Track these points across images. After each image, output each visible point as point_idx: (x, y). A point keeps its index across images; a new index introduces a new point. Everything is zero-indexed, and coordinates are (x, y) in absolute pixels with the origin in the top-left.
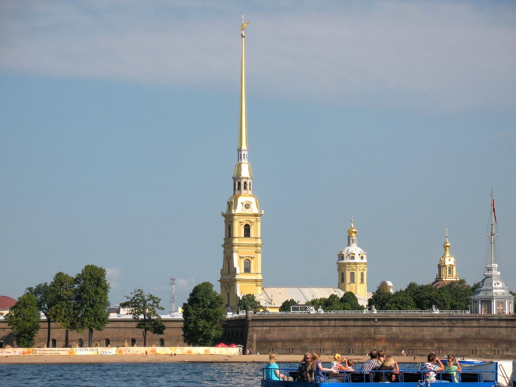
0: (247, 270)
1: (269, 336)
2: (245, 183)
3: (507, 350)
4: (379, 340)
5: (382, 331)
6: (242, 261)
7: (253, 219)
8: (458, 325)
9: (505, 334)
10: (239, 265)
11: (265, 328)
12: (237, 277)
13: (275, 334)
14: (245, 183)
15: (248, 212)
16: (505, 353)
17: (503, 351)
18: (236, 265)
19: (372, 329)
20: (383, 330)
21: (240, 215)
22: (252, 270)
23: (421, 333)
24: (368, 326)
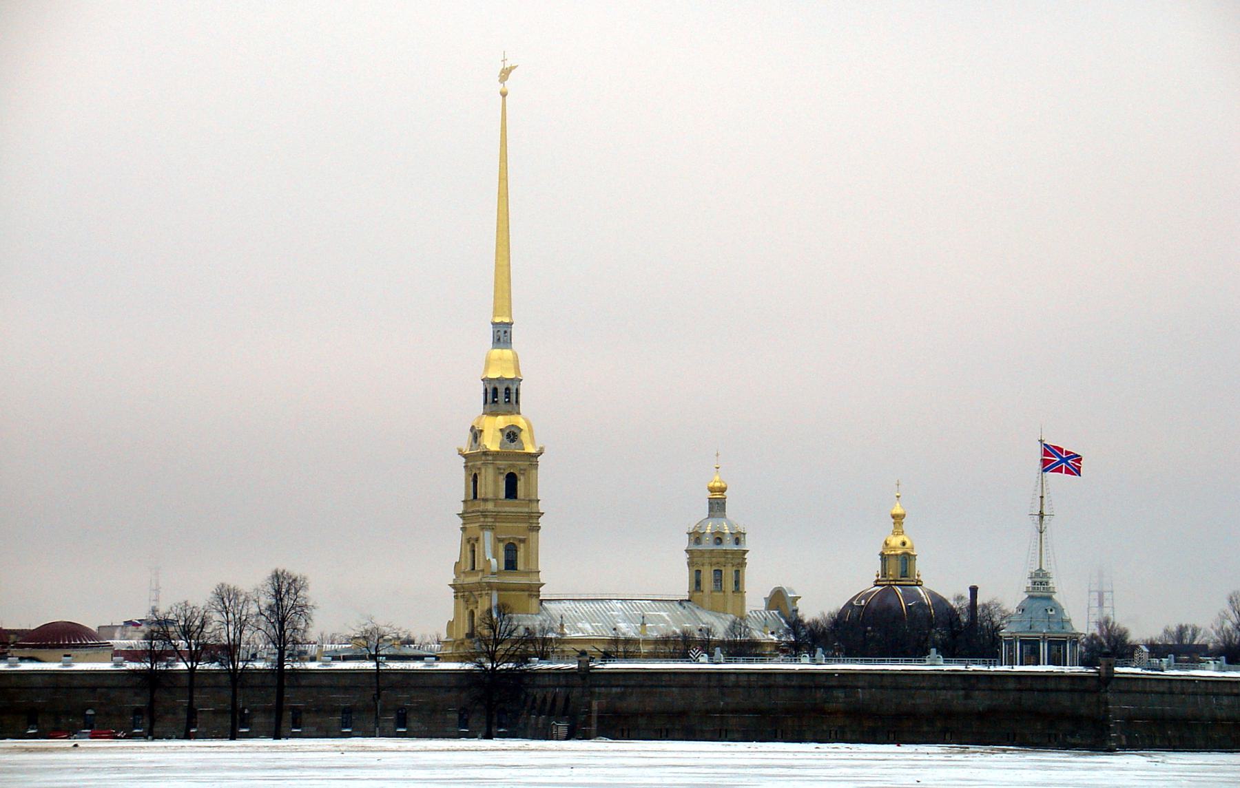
0: (511, 564)
1: (623, 705)
2: (507, 389)
3: (1072, 734)
4: (834, 713)
5: (838, 698)
6: (501, 547)
7: (523, 464)
8: (981, 685)
9: (1068, 704)
10: (495, 556)
11: (614, 690)
12: (494, 580)
13: (633, 702)
14: (507, 389)
15: (512, 448)
16: (1069, 739)
17: (1065, 735)
18: (489, 556)
19: (820, 694)
20: (840, 694)
21: (496, 455)
22: (520, 566)
23: (910, 702)
24: (811, 687)
